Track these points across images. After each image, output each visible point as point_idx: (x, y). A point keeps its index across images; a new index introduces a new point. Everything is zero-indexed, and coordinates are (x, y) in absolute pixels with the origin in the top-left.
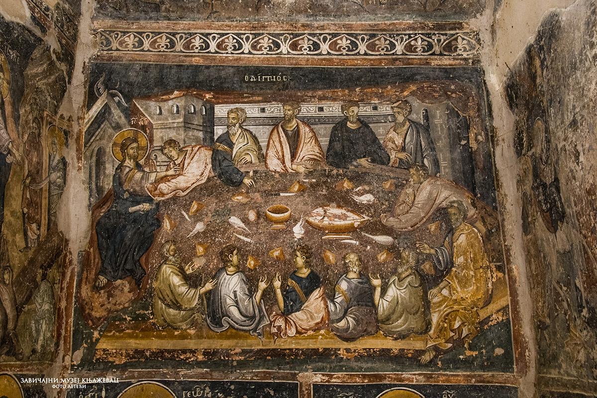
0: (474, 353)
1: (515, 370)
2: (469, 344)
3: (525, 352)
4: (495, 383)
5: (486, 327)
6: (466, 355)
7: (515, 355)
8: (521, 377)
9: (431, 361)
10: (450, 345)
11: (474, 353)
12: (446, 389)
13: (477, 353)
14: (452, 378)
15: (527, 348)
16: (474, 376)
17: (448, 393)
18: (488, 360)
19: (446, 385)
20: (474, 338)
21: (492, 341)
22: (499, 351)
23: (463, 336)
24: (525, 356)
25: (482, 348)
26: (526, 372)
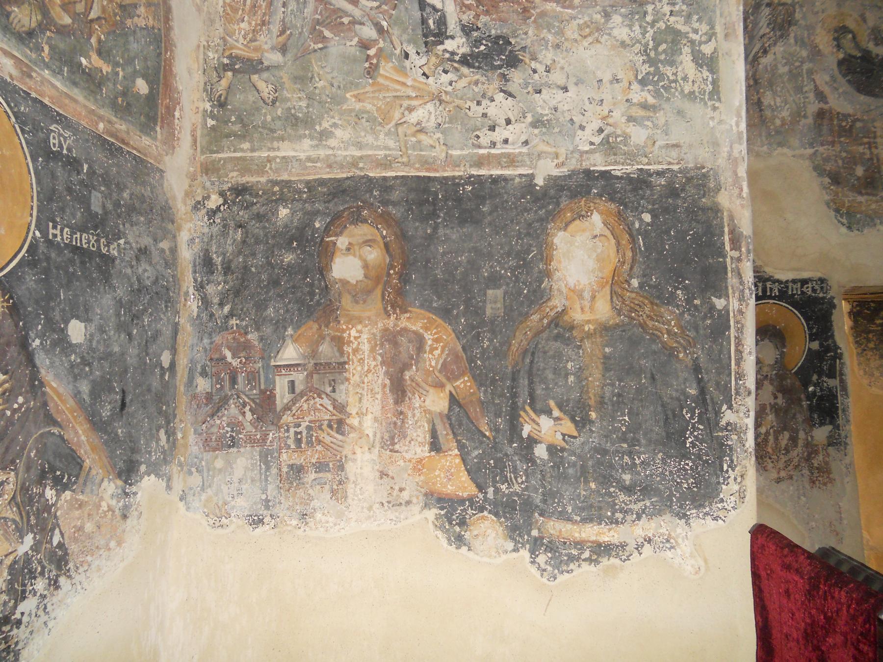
0: (106, 69)
1: (159, 136)
2: (99, 41)
3: (174, 110)
4: (135, 149)
5: (129, 22)
6: (90, 63)
7: (162, 110)
8: (167, 155)
9: (31, 34)
10: (67, 20)
11: (106, 69)
12: (57, 122)
13: (109, 70)
14: (67, 101)
15: (179, 103)
16: (101, 118)
17: (60, 135)
18: (124, 94)
19: (59, 114)
20: (109, 34)
21: (135, 58)
22: (142, 86)
23: (93, 15)
24: (174, 116)
25: (117, 64)
26: (174, 148)
